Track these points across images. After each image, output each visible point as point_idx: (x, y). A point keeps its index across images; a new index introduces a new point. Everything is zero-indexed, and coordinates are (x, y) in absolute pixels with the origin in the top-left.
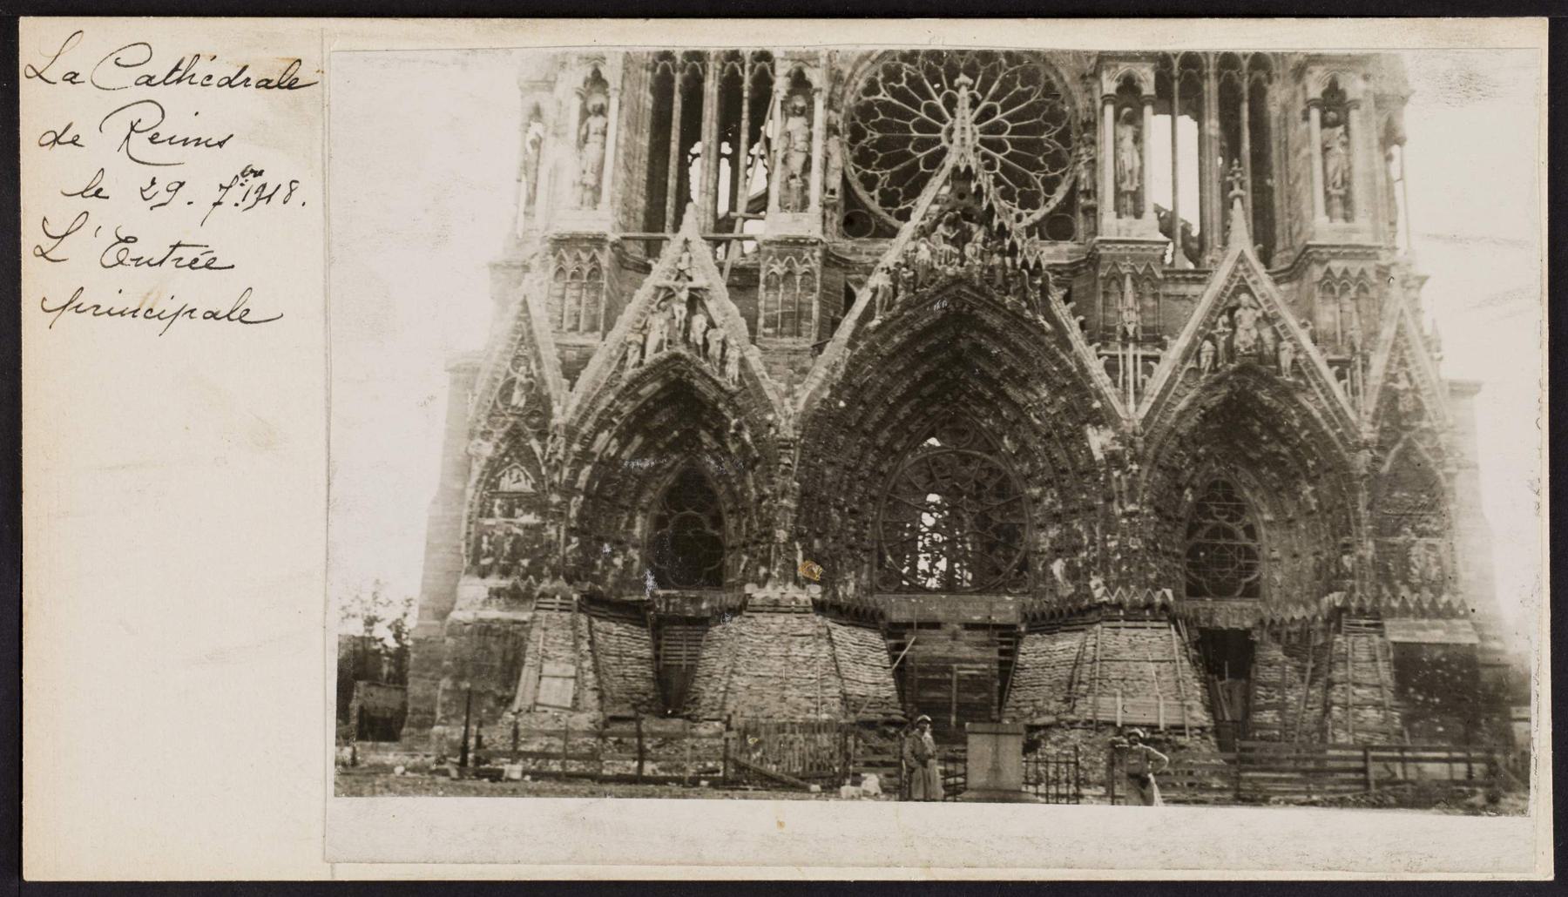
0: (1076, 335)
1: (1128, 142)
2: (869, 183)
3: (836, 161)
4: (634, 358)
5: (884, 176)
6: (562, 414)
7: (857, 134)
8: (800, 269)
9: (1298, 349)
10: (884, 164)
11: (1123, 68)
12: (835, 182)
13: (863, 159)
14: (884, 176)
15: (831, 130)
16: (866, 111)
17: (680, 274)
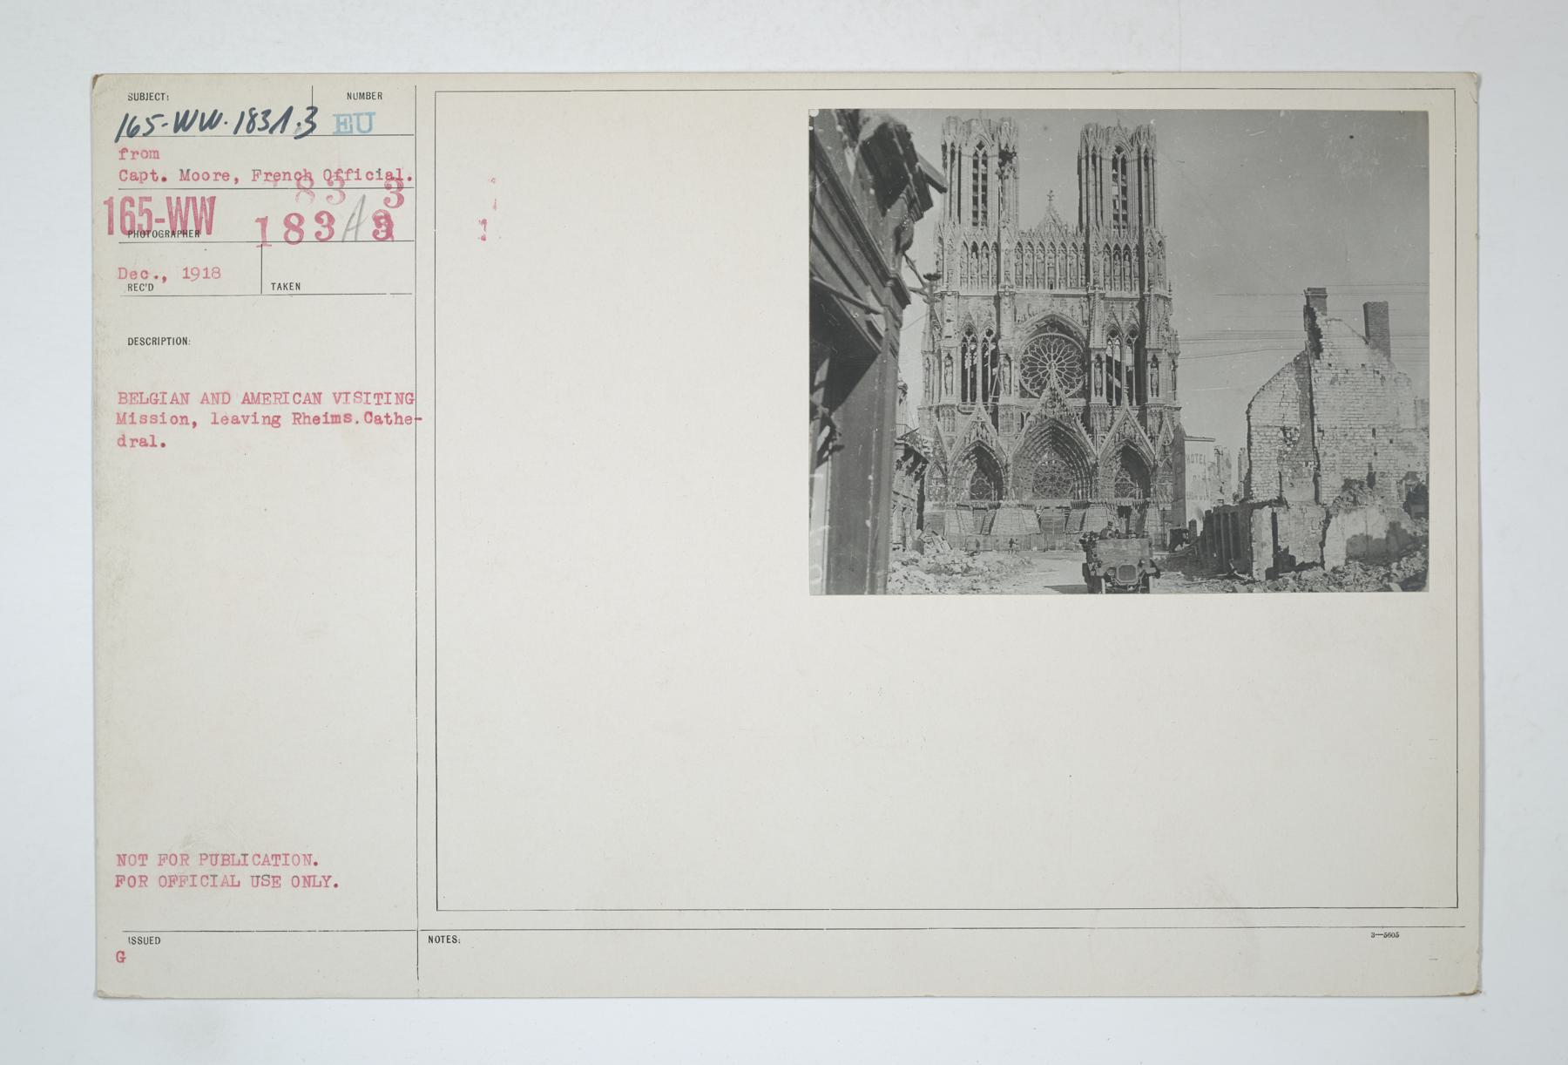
0: (1084, 432)
1: (1098, 374)
2: (1026, 381)
3: (1017, 378)
4: (968, 441)
5: (1031, 379)
6: (949, 458)
7: (1022, 367)
8: (1009, 413)
9: (1141, 434)
10: (1031, 376)
11: (1097, 353)
12: (1018, 384)
13: (1025, 374)
14: (1031, 379)
15: (1016, 368)
16: (1024, 360)
17: (978, 418)
